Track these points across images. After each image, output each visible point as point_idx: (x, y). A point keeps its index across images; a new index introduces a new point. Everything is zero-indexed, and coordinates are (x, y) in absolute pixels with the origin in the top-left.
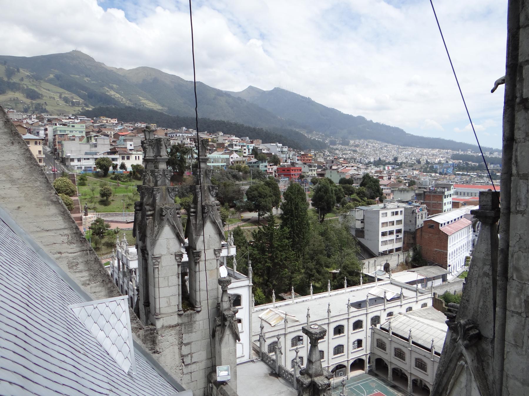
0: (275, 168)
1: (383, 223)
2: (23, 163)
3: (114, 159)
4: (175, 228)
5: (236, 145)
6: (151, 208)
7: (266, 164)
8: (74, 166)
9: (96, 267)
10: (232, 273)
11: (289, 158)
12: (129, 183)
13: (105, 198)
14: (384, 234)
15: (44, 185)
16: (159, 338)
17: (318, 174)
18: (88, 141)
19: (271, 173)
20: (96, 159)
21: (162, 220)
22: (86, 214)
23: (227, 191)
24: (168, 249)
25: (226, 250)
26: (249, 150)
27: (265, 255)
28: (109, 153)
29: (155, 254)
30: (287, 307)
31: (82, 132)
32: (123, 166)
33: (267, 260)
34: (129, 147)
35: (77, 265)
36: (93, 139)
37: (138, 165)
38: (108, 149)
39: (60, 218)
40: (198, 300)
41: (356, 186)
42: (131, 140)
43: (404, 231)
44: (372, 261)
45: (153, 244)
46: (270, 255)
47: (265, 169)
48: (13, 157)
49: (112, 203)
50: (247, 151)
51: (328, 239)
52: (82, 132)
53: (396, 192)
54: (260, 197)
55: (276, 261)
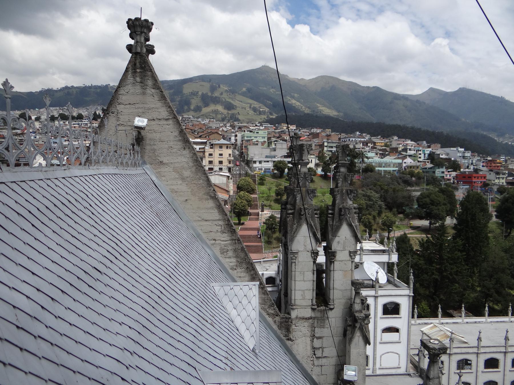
0: (454, 174)
2: (191, 164)
4: (312, 227)
5: (410, 150)
6: (291, 208)
7: (444, 170)
8: (256, 168)
9: (242, 255)
10: (392, 280)
11: (472, 164)
13: (279, 197)
15: (206, 183)
16: (293, 327)
18: (269, 146)
19: (449, 180)
20: (274, 162)
21: (301, 219)
22: (262, 211)
24: (305, 246)
26: (425, 154)
28: (285, 157)
29: (293, 249)
30: (455, 325)
31: (264, 138)
33: (434, 271)
35: (227, 251)
36: (273, 143)
39: (216, 211)
40: (331, 297)
45: (292, 240)
46: (438, 267)
47: (442, 175)
48: (184, 160)
50: (422, 156)
52: (264, 138)
54: (433, 205)
55: (445, 274)
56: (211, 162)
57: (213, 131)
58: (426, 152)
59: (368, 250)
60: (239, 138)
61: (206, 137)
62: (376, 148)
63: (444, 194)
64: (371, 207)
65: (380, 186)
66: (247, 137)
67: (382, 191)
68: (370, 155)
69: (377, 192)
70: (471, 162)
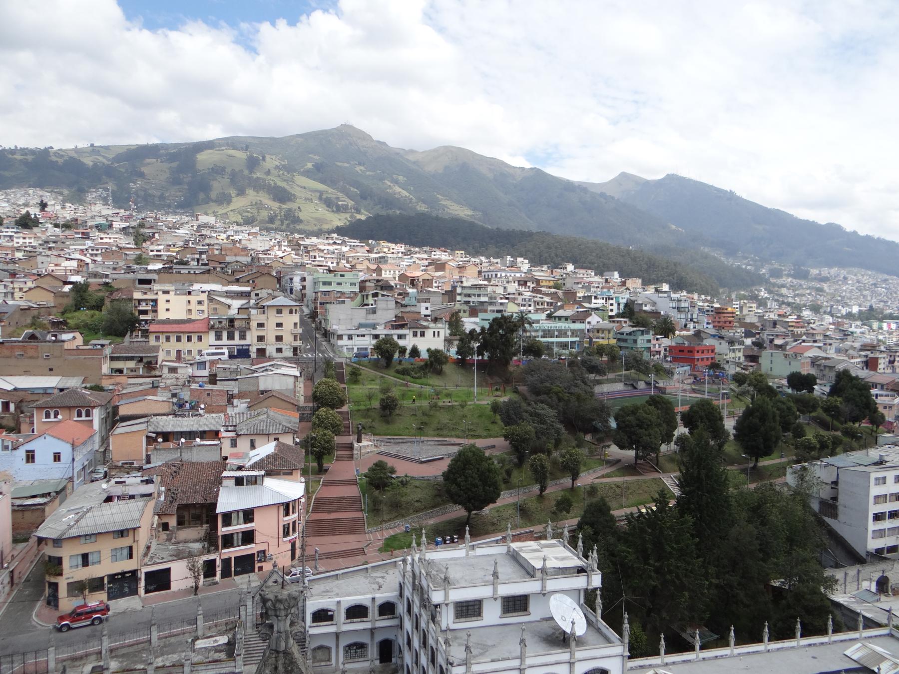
0: (666, 342)
1: (877, 497)
5: (596, 298)
8: (342, 346)
10: (593, 619)
11: (691, 320)
12: (423, 380)
14: (878, 517)
19: (658, 352)
20: (376, 337)
22: (359, 441)
26: (619, 304)
27: (649, 564)
32: (415, 352)
33: (653, 574)
38: (390, 316)
41: (821, 390)
44: (852, 571)
47: (648, 345)
54: (640, 426)
56: (261, 339)
57: (260, 270)
58: (621, 301)
60: (308, 283)
61: (248, 281)
65: (556, 394)
66: (325, 283)
67: (561, 404)
68: (533, 317)
69: (552, 407)
70: (689, 316)
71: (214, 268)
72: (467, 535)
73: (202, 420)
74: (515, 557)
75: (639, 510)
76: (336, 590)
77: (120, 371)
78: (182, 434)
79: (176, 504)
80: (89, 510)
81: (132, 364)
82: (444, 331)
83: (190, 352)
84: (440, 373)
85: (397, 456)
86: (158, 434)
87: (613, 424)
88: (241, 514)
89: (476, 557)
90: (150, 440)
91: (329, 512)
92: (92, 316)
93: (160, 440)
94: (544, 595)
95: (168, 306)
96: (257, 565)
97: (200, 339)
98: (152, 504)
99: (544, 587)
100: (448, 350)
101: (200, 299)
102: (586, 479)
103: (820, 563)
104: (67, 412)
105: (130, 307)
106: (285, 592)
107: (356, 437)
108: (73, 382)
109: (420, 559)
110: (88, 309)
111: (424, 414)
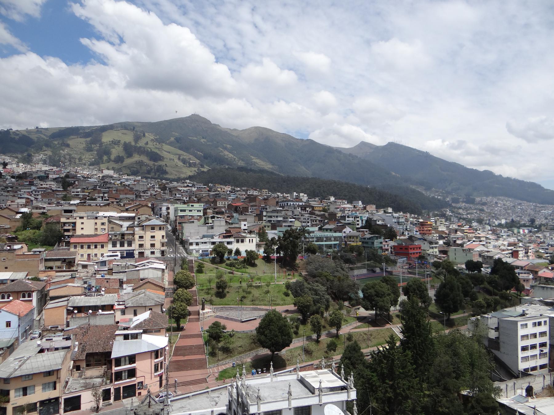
0: (392, 243)
1: (523, 337)
3: (229, 243)
5: (348, 217)
7: (382, 240)
8: (192, 250)
11: (406, 229)
12: (244, 270)
13: (221, 290)
14: (524, 349)
17: (441, 252)
19: (387, 250)
20: (213, 243)
22: (203, 309)
23: (342, 286)
25: (346, 394)
26: (362, 221)
28: (225, 237)
32: (238, 252)
33: (389, 389)
34: (243, 227)
36: (210, 219)
37: (252, 251)
41: (486, 270)
42: (245, 220)
43: (550, 345)
44: (510, 383)
46: (391, 383)
47: (381, 245)
49: (228, 295)
50: (360, 222)
51: (456, 354)
53: (537, 288)
55: (398, 391)
56: (141, 246)
57: (141, 203)
58: (363, 219)
59: (326, 388)
60: (172, 211)
61: (134, 210)
62: (314, 214)
63: (387, 284)
64: (318, 302)
65: (325, 276)
66: (181, 211)
68: (311, 229)
69: (323, 285)
70: (405, 227)
71: (113, 202)
72: (272, 368)
73: (103, 298)
74: (302, 381)
75: (378, 349)
76: (188, 407)
77: (51, 268)
78: (90, 307)
79: (85, 353)
80: (28, 359)
81: (59, 263)
82: (256, 240)
83: (96, 255)
84: (254, 265)
85: (227, 318)
86: (75, 308)
87: (361, 295)
88: (127, 358)
89: (277, 382)
90: (69, 312)
91: (184, 355)
92: (34, 233)
93: (76, 312)
94: (321, 405)
95: (82, 226)
96: (137, 392)
97: (102, 247)
98: (69, 356)
99: (320, 401)
100: (258, 251)
101: (103, 221)
102: (345, 330)
103: (491, 379)
104: (16, 295)
105: (58, 227)
106: (151, 410)
107: (201, 306)
108: (20, 276)
109: (241, 385)
110: (31, 229)
111: (244, 291)
